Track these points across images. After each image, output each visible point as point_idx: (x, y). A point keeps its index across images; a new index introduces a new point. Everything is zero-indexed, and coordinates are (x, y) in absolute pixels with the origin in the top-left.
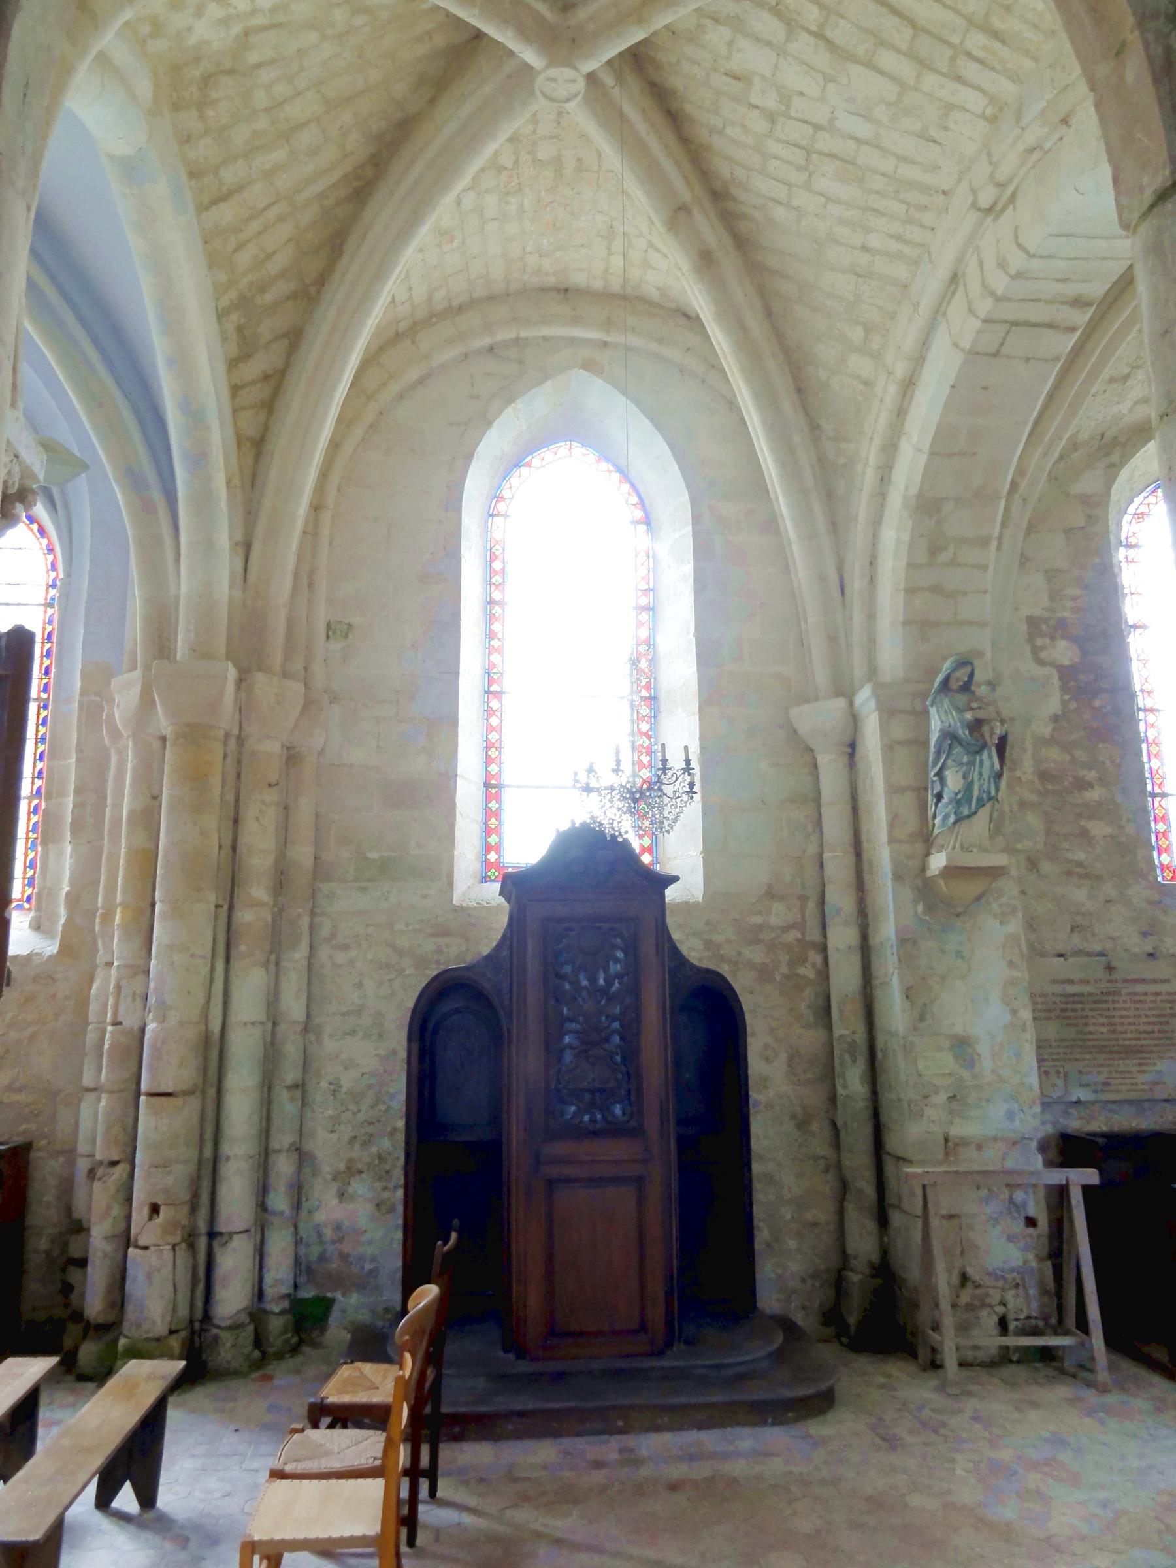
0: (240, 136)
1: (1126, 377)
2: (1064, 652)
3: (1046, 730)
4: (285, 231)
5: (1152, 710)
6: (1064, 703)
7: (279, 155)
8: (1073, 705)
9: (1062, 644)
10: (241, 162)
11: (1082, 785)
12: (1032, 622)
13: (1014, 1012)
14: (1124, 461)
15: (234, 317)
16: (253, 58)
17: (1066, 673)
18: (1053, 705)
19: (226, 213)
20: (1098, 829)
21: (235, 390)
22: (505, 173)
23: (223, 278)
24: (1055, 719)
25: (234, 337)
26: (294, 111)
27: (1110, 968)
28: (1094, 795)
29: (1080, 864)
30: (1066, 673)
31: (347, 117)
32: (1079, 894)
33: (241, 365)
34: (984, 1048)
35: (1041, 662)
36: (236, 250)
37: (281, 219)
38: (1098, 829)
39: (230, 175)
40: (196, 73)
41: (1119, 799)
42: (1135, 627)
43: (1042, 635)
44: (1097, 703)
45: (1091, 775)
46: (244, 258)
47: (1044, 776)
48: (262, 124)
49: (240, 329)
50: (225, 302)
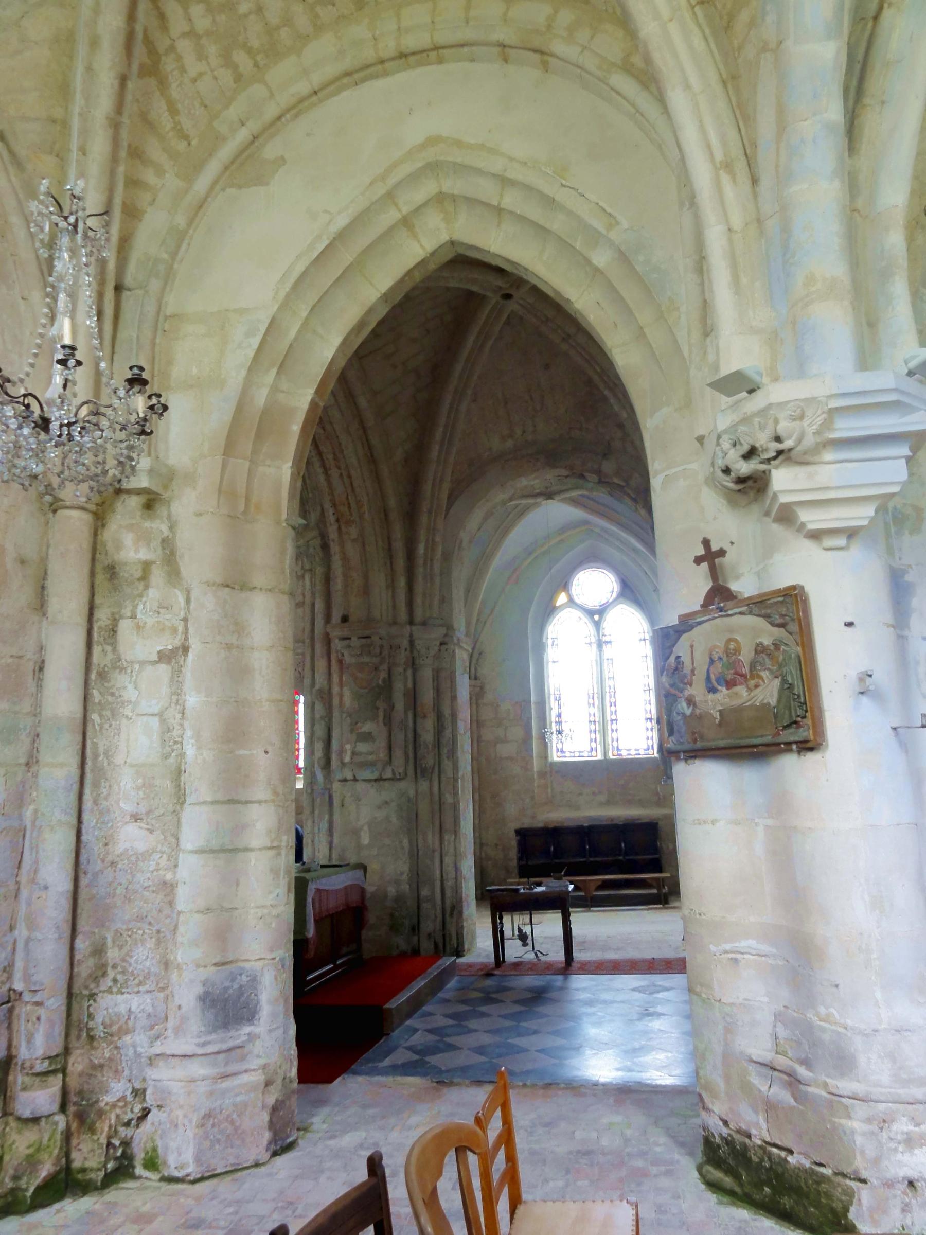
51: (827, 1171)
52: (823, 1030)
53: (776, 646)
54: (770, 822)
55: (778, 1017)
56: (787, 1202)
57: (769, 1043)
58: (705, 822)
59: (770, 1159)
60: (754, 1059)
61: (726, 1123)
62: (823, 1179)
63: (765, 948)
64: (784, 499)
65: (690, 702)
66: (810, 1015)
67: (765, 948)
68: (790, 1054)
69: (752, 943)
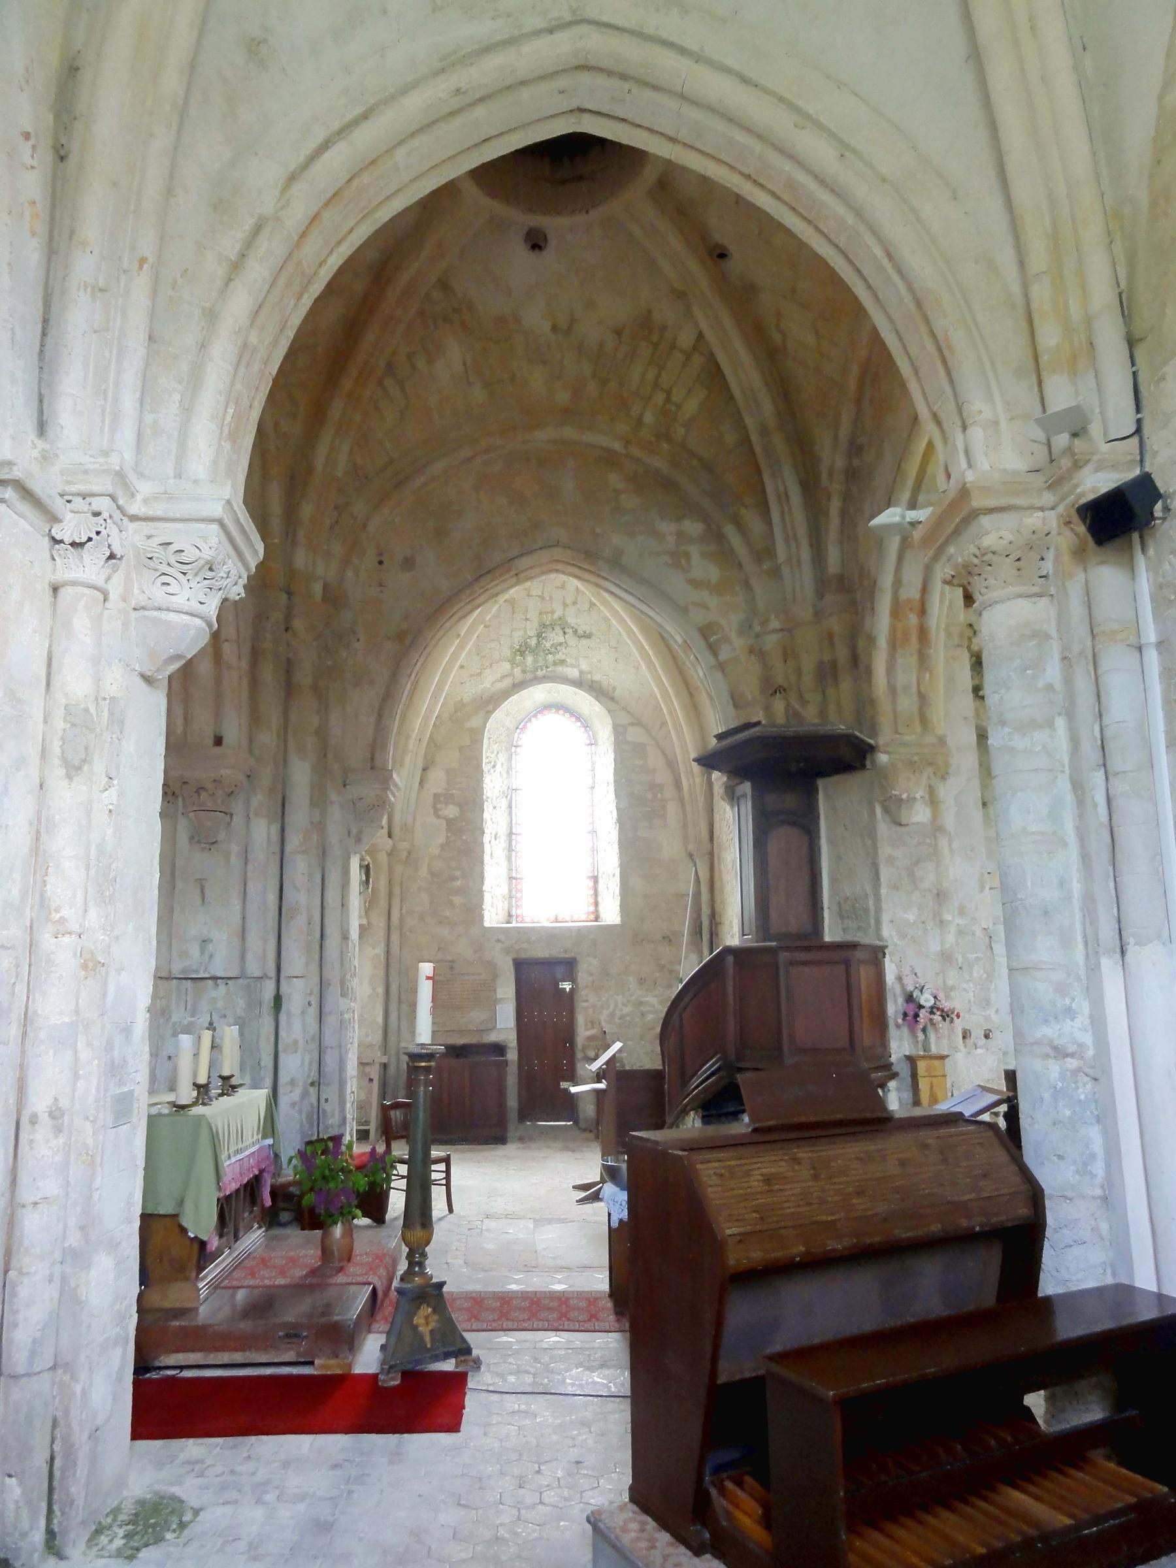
1: (480, 674)
2: (451, 811)
3: (437, 852)
5: (519, 834)
6: (447, 837)
8: (453, 838)
9: (451, 806)
11: (453, 878)
12: (436, 796)
13: (374, 989)
14: (494, 710)
17: (450, 822)
18: (441, 839)
20: (458, 900)
24: (442, 846)
27: (452, 968)
28: (458, 883)
29: (447, 917)
30: (450, 822)
32: (445, 932)
35: (438, 817)
38: (458, 900)
41: (471, 884)
42: (516, 790)
43: (441, 802)
44: (464, 837)
45: (458, 873)
47: (433, 874)
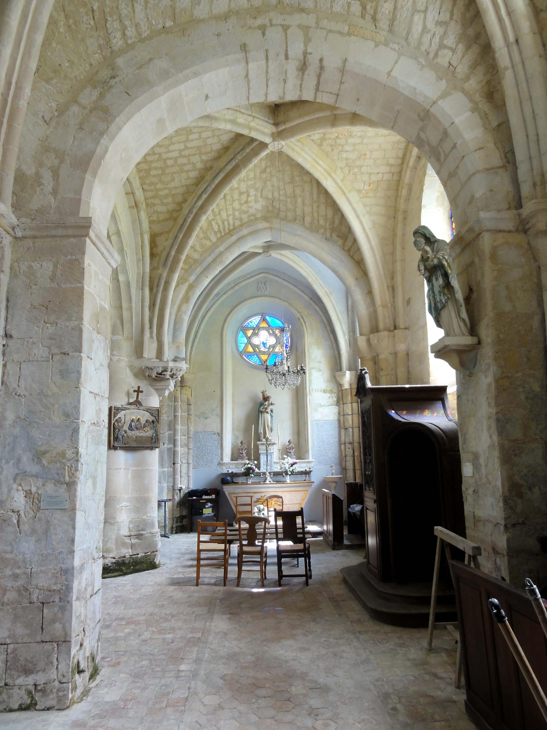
0: (290, 206)
4: (322, 207)
7: (299, 200)
10: (297, 209)
13: (491, 437)
15: (334, 235)
16: (270, 196)
19: (308, 219)
21: (349, 251)
22: (340, 136)
23: (322, 230)
25: (338, 239)
26: (289, 191)
31: (297, 179)
33: (346, 243)
34: (482, 461)
36: (318, 222)
37: (318, 207)
39: (299, 212)
40: (271, 208)
46: (322, 222)
48: (289, 200)
49: (338, 236)
50: (328, 235)
51: (149, 553)
52: (149, 520)
53: (153, 422)
54: (134, 469)
55: (130, 522)
56: (138, 567)
57: (127, 530)
58: (119, 469)
59: (133, 559)
60: (126, 535)
61: (114, 558)
62: (149, 555)
63: (128, 504)
64: (170, 387)
65: (126, 432)
66: (144, 517)
67: (128, 504)
68: (134, 530)
69: (125, 503)
